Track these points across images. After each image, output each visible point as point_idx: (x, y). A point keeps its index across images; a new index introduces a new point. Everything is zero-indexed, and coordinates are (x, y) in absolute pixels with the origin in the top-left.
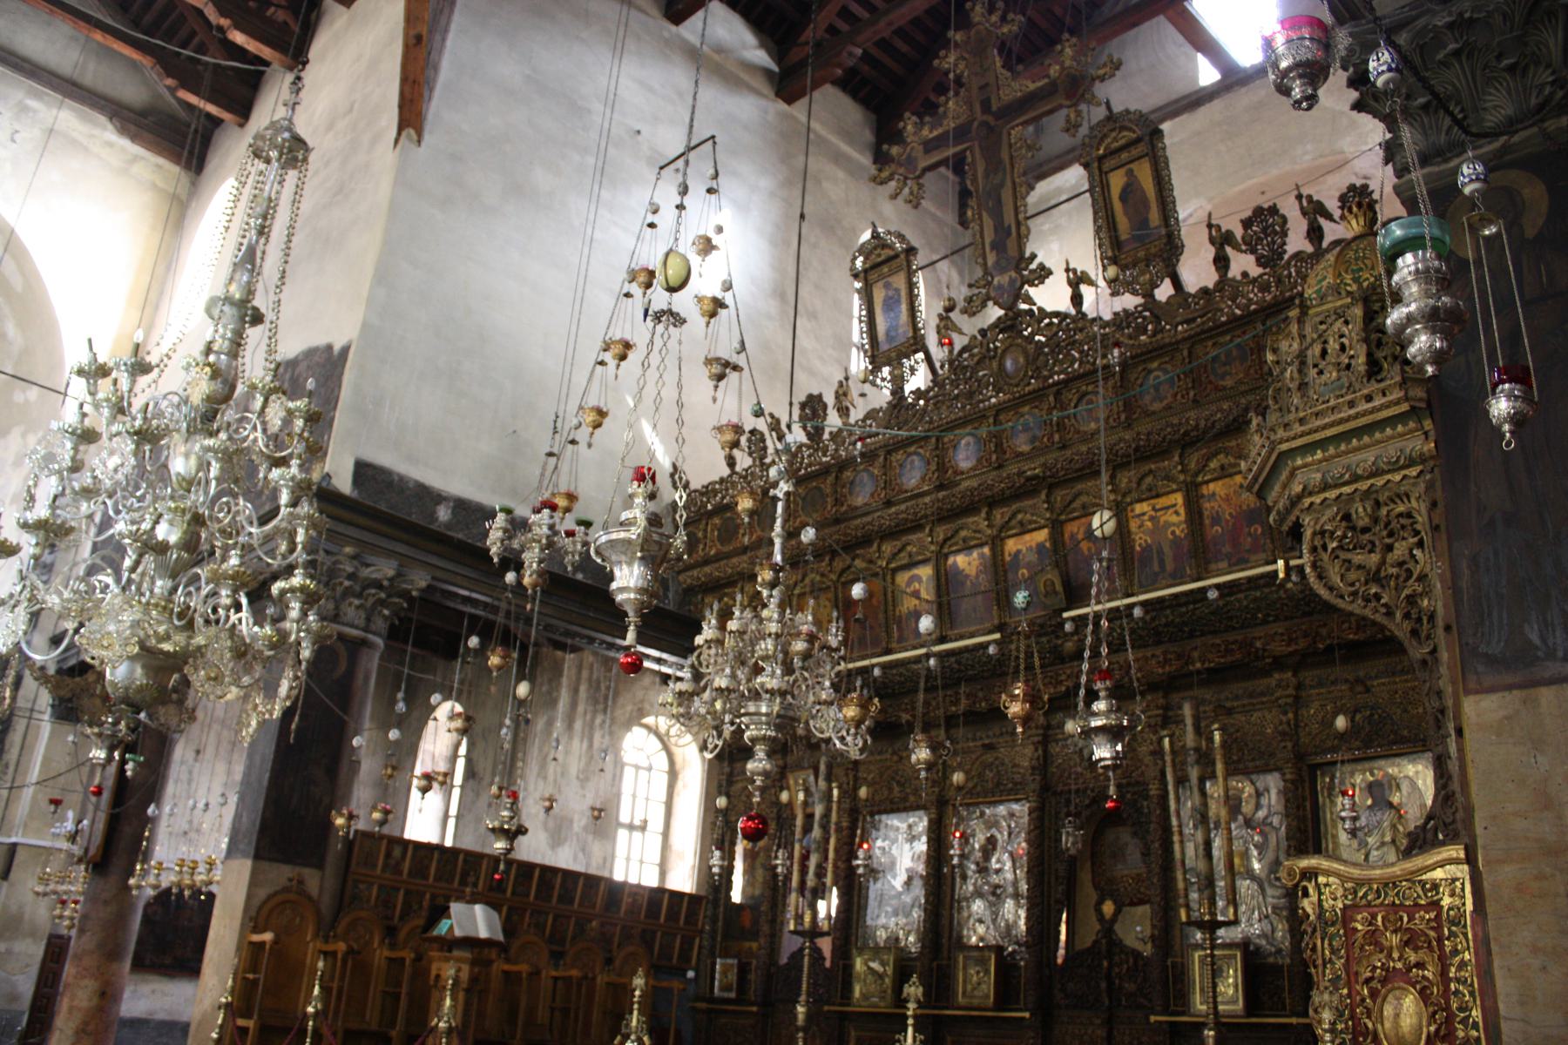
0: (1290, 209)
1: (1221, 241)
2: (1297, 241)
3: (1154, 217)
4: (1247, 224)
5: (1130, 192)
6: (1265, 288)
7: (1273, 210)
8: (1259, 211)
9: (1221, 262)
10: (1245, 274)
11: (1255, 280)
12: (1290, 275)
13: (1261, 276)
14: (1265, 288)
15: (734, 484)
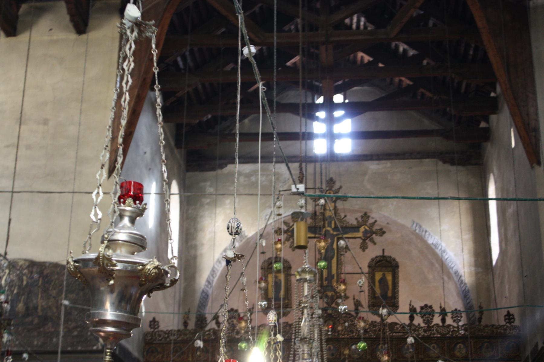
0: (437, 309)
1: (413, 310)
2: (437, 320)
3: (390, 294)
4: (422, 308)
5: (383, 281)
6: (425, 331)
7: (431, 307)
8: (426, 306)
9: (412, 318)
10: (419, 324)
11: (422, 328)
12: (433, 330)
13: (425, 327)
14: (425, 331)
15: (185, 334)
